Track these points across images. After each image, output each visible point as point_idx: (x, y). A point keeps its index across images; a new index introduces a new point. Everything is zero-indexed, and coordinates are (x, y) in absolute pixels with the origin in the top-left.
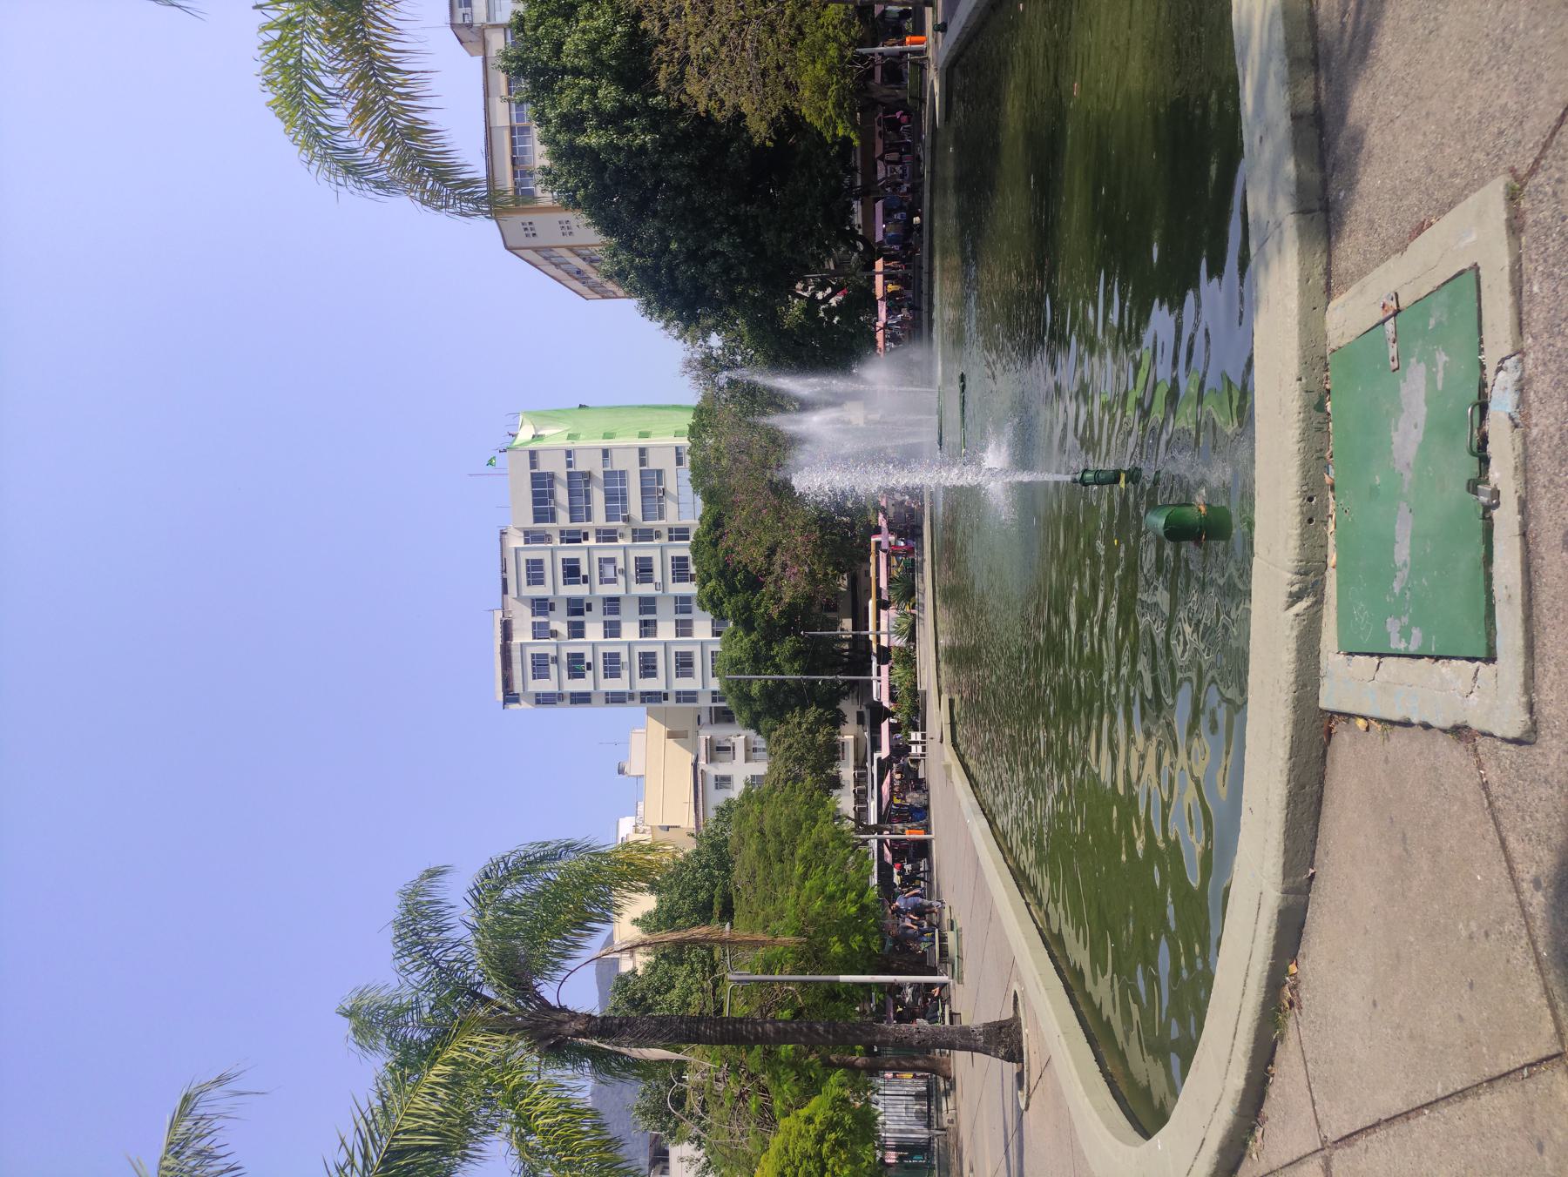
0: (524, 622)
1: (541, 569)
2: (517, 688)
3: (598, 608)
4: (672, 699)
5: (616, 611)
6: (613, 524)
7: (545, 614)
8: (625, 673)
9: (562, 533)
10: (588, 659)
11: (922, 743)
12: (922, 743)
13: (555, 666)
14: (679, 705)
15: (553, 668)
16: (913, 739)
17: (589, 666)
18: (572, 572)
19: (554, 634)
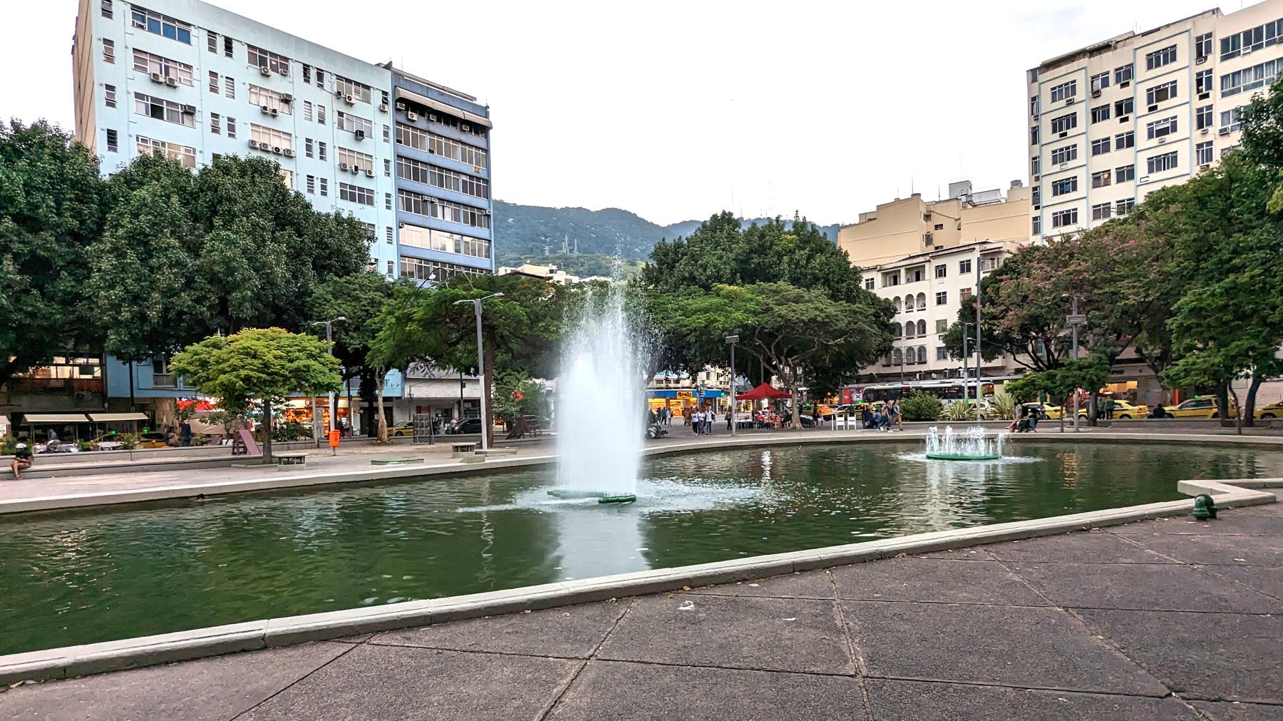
0: (1108, 63)
1: (1166, 62)
2: (1042, 78)
3: (1125, 128)
4: (1037, 213)
5: (1120, 145)
6: (1217, 119)
7: (1117, 82)
8: (1057, 167)
9: (1210, 71)
10: (1071, 132)
11: (846, 426)
12: (846, 426)
13: (1065, 105)
14: (1031, 220)
15: (1063, 102)
16: (849, 418)
17: (1065, 134)
18: (1160, 94)
19: (1096, 94)
